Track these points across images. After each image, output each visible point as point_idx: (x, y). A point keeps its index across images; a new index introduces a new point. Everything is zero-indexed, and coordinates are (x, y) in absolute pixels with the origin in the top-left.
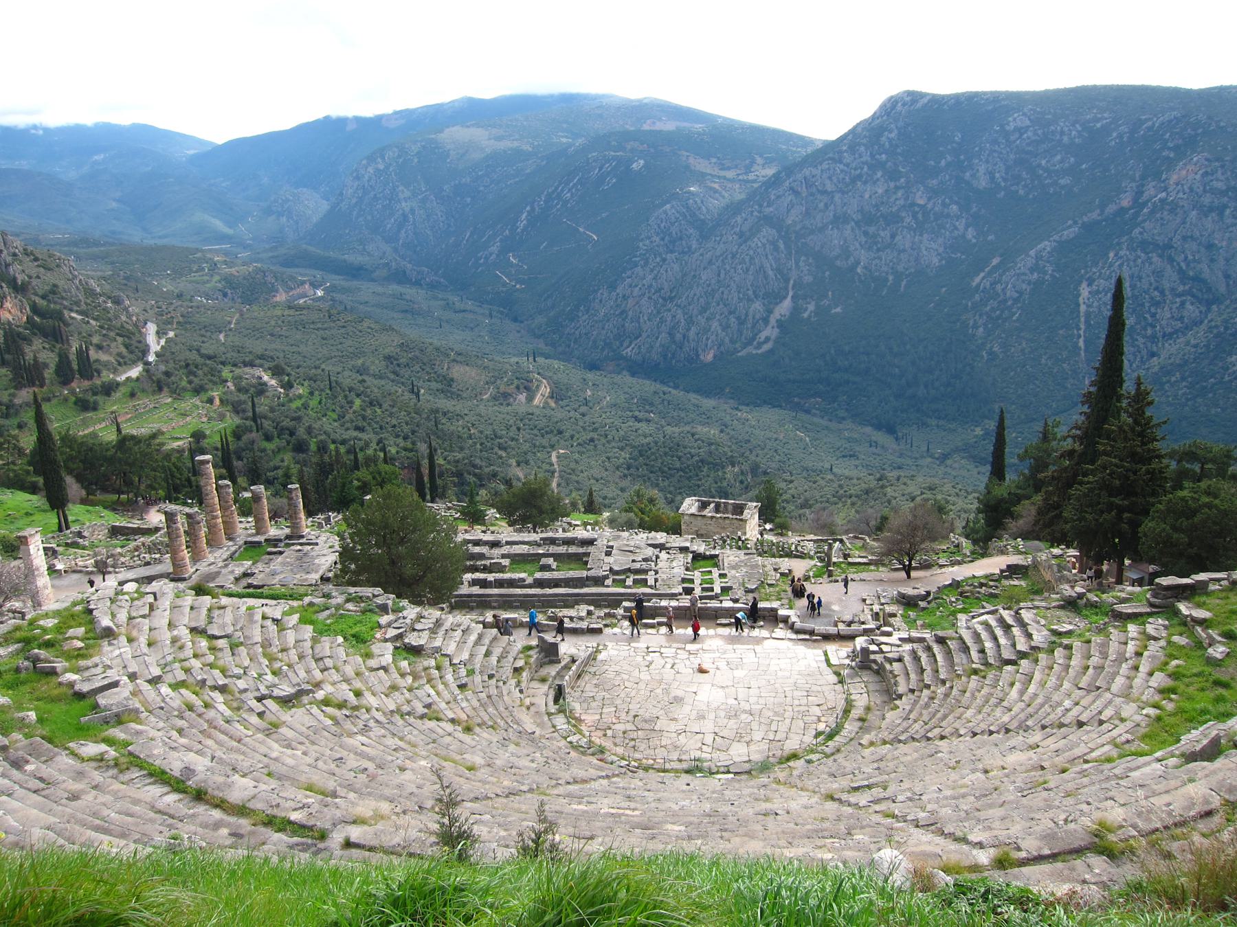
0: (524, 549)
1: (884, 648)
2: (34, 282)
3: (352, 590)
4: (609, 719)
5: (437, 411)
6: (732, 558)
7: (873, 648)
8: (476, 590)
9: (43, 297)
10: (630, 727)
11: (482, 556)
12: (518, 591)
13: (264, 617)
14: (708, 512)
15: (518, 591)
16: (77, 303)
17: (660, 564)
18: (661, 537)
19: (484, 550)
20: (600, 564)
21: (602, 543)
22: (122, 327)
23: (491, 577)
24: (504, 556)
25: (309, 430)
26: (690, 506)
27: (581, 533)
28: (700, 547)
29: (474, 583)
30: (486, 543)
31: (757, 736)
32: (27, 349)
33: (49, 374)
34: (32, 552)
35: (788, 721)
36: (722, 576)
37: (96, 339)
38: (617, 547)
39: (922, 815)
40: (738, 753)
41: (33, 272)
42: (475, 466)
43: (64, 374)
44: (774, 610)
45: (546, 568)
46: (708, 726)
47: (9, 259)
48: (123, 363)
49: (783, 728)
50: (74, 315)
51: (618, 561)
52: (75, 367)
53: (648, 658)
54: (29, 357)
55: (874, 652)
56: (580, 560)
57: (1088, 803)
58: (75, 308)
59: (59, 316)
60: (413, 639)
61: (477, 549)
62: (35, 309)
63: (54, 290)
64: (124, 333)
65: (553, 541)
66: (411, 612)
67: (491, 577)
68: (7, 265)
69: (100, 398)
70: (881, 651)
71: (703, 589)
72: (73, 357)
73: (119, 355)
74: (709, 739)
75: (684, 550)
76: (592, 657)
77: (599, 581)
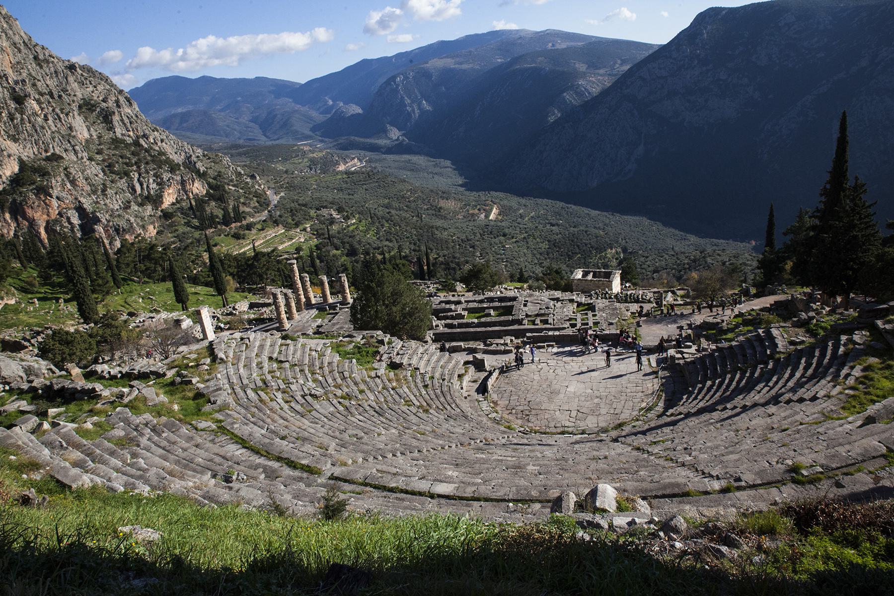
0: (475, 305)
1: (686, 356)
3: (365, 332)
4: (513, 403)
5: (432, 227)
6: (600, 305)
7: (679, 356)
8: (447, 330)
9: (214, 179)
10: (526, 407)
11: (450, 310)
12: (472, 330)
13: (310, 350)
14: (590, 277)
15: (472, 330)
16: (232, 181)
17: (557, 310)
18: (558, 294)
19: (453, 307)
20: (521, 311)
21: (521, 299)
23: (455, 322)
24: (463, 309)
25: (360, 242)
27: (511, 294)
28: (583, 299)
29: (446, 326)
30: (453, 302)
31: (603, 411)
35: (623, 402)
36: (594, 316)
37: (242, 200)
38: (530, 301)
39: (689, 458)
40: (591, 423)
41: (208, 166)
42: (455, 258)
45: (489, 315)
46: (574, 406)
47: (195, 159)
48: (257, 211)
49: (620, 406)
51: (531, 309)
52: (232, 215)
55: (679, 359)
56: (508, 311)
57: (795, 451)
60: (397, 360)
61: (448, 306)
62: (210, 186)
63: (220, 175)
64: (257, 195)
65: (491, 300)
66: (398, 343)
67: (455, 322)
68: (195, 163)
70: (684, 358)
71: (583, 324)
72: (230, 211)
73: (255, 207)
74: (574, 414)
75: (572, 301)
77: (520, 322)
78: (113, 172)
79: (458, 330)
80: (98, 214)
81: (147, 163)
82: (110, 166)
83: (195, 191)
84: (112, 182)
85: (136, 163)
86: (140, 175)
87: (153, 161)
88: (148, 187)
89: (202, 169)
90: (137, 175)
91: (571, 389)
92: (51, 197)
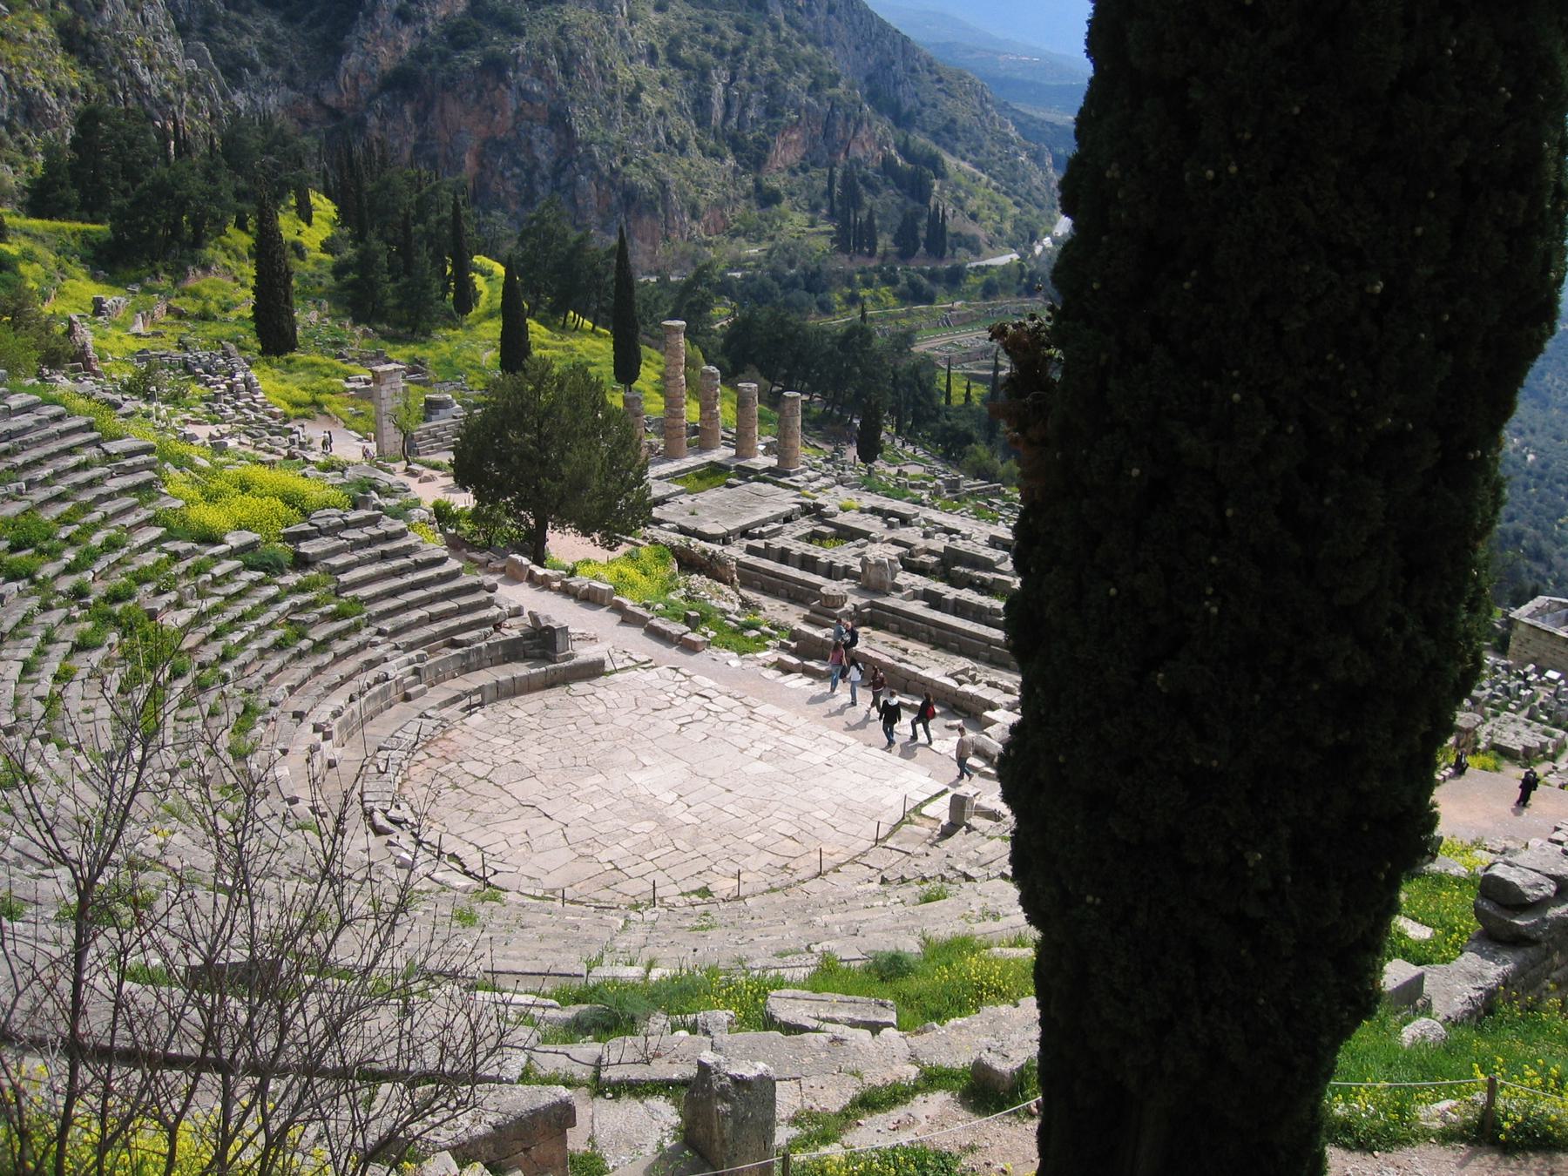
2: (927, 112)
22: (1029, 194)
23: (951, 593)
26: (1540, 612)
31: (603, 857)
32: (867, 200)
33: (884, 242)
34: (384, 394)
37: (972, 204)
41: (928, 99)
43: (906, 243)
44: (992, 706)
50: (965, 166)
52: (922, 234)
53: (677, 702)
54: (863, 215)
58: (970, 156)
59: (934, 163)
67: (951, 593)
68: (897, 83)
69: (939, 290)
73: (1000, 232)
76: (594, 670)
78: (675, 61)
79: (938, 616)
80: (596, 150)
81: (762, 55)
82: (675, 43)
83: (858, 152)
84: (664, 82)
85: (736, 52)
86: (733, 79)
87: (779, 55)
88: (742, 113)
89: (908, 104)
90: (725, 74)
91: (638, 778)
92: (509, 87)
